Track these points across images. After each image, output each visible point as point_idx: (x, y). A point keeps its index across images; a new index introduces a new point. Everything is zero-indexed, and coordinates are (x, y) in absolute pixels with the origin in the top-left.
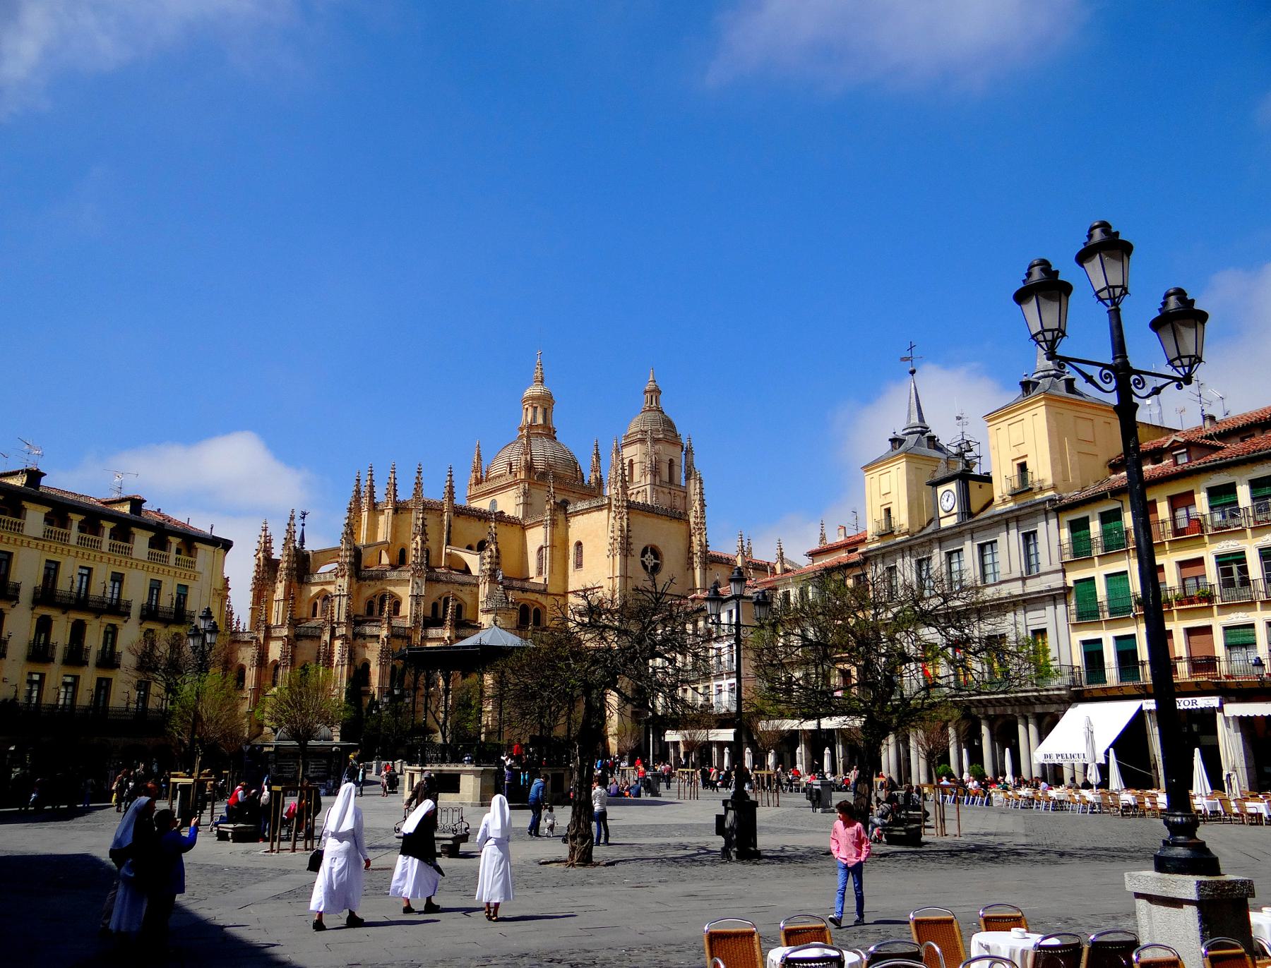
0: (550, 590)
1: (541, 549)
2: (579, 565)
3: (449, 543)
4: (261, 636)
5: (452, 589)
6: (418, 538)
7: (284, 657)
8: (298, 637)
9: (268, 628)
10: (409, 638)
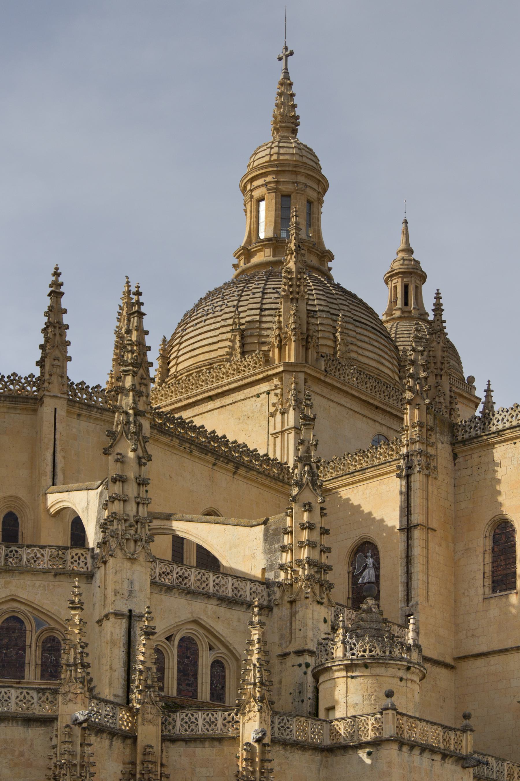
5: (206, 611)
10: (130, 737)
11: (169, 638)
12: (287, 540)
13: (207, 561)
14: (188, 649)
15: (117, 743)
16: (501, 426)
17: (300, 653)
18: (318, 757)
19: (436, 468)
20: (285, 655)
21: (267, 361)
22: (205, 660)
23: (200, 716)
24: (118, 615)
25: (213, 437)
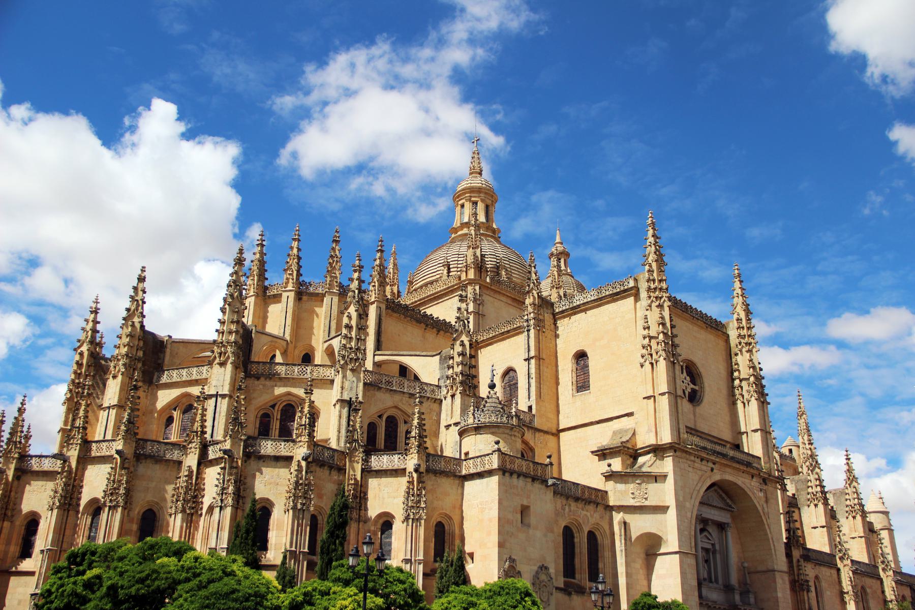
0: (537, 423)
1: (509, 372)
2: (582, 385)
3: (378, 346)
4: (73, 454)
6: (352, 310)
7: (111, 492)
8: (139, 457)
9: (86, 444)
10: (341, 470)
11: (380, 417)
12: (451, 362)
13: (416, 378)
14: (392, 423)
15: (334, 473)
16: (578, 303)
17: (456, 424)
18: (457, 482)
19: (544, 327)
20: (448, 427)
21: (460, 278)
22: (402, 428)
23: (385, 458)
24: (341, 401)
25: (425, 315)
